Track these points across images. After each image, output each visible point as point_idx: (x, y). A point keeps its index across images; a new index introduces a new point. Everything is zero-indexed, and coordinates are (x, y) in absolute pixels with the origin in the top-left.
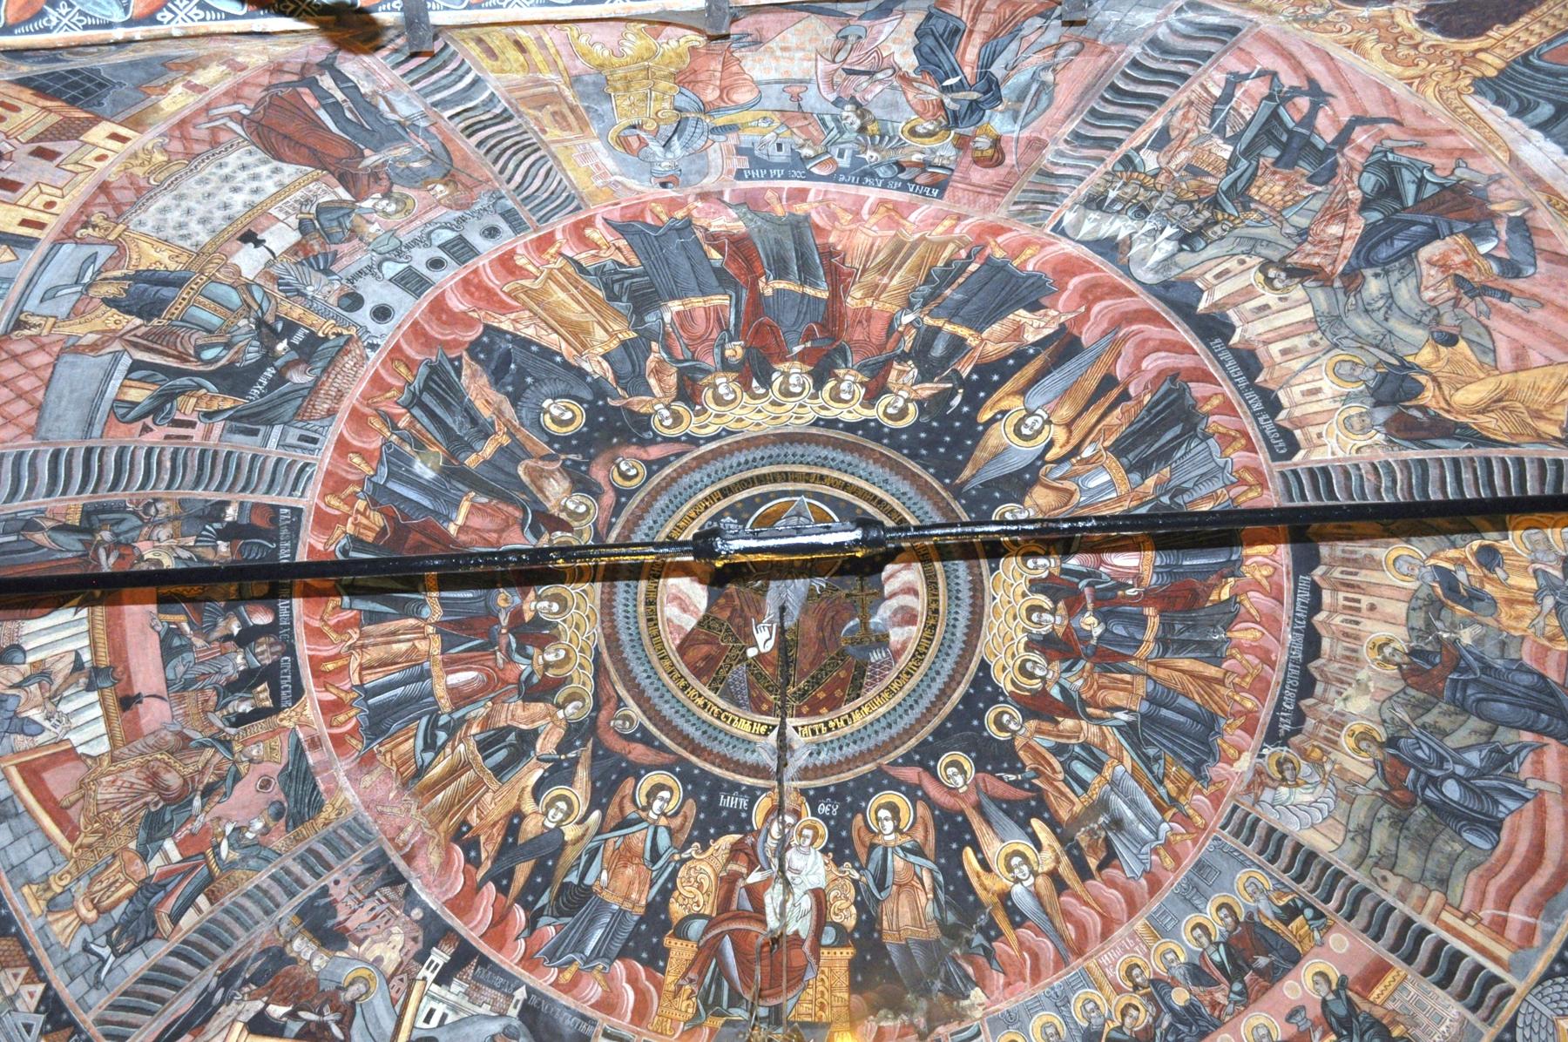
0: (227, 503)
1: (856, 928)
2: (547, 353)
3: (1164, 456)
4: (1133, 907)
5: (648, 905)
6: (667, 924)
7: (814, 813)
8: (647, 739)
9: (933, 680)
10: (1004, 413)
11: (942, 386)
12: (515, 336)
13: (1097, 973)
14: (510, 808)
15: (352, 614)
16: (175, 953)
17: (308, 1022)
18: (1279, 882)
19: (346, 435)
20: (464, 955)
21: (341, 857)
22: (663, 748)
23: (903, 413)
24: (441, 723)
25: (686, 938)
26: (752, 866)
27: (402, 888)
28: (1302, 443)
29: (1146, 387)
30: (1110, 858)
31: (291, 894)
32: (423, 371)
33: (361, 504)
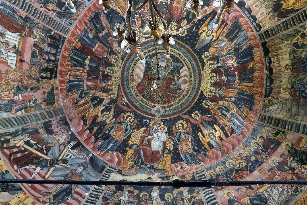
0: (52, 31)
1: (173, 150)
2: (117, 13)
3: (236, 37)
4: (239, 142)
5: (124, 141)
6: (128, 145)
7: (164, 125)
8: (127, 106)
9: (191, 96)
10: (203, 31)
11: (191, 25)
12: (112, 9)
13: (232, 157)
14: (95, 114)
15: (71, 63)
16: (13, 118)
17: (39, 147)
18: (273, 128)
19: (77, 24)
20: (79, 145)
21: (56, 115)
22: (131, 108)
23: (184, 32)
24: (84, 92)
25: (132, 149)
26: (149, 134)
27: (68, 126)
28: (262, 26)
29: (230, 22)
30: (233, 131)
31: (43, 119)
32: (94, 14)
33: (77, 40)
